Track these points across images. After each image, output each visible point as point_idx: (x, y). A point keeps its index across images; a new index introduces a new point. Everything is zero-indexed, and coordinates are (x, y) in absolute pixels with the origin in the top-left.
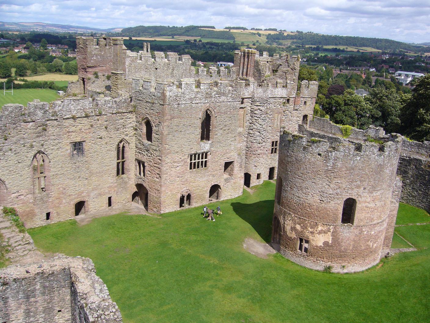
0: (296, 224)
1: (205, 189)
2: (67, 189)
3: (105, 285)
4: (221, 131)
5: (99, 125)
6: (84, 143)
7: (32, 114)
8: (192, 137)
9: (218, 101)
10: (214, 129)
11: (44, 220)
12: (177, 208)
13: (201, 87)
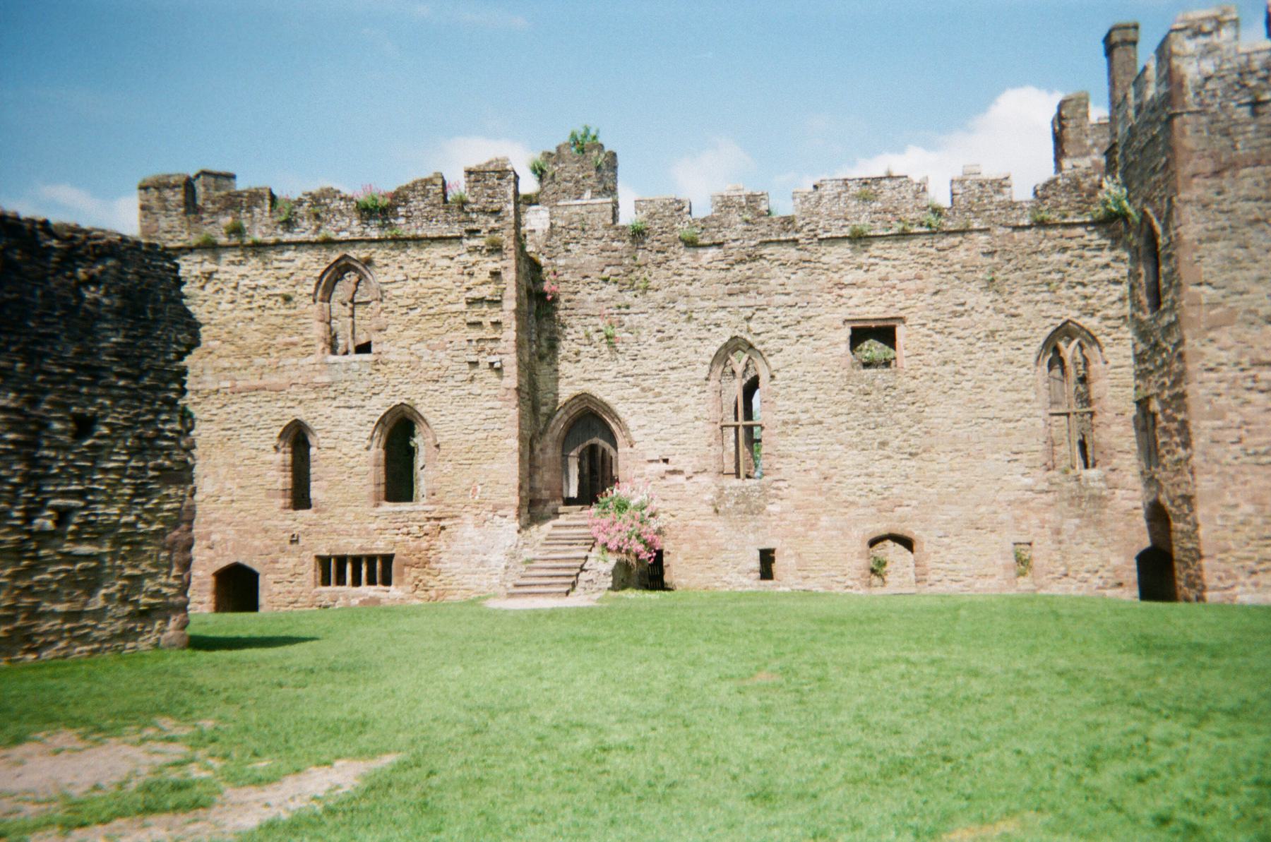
2: (835, 479)
5: (957, 267)
7: (716, 224)
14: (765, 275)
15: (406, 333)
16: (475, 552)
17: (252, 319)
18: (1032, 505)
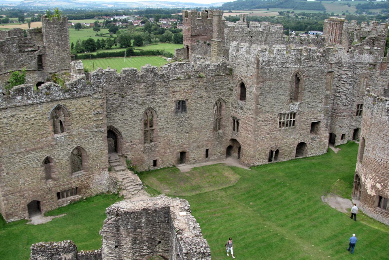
0: (376, 183)
1: (293, 146)
2: (171, 141)
3: (198, 224)
4: (309, 94)
5: (199, 86)
6: (187, 102)
7: (144, 76)
8: (282, 98)
9: (307, 66)
10: (302, 92)
11: (152, 166)
12: (266, 161)
13: (292, 53)
14: (157, 90)
15: (77, 126)
16: (98, 181)
17: (30, 128)
18: (210, 140)
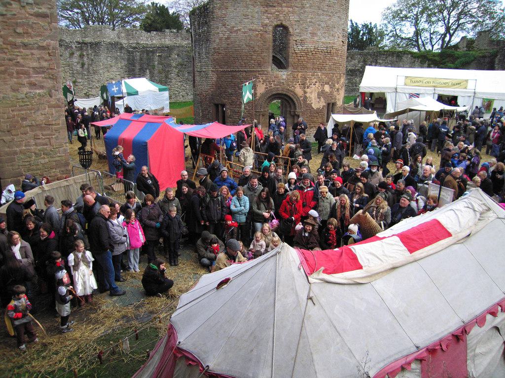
0: (324, 85)
